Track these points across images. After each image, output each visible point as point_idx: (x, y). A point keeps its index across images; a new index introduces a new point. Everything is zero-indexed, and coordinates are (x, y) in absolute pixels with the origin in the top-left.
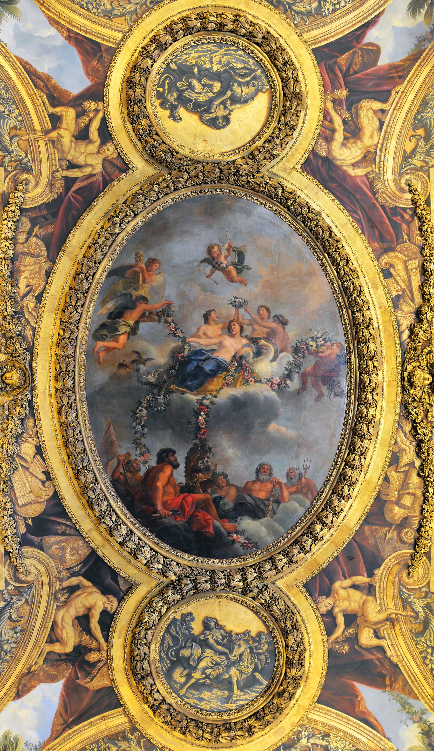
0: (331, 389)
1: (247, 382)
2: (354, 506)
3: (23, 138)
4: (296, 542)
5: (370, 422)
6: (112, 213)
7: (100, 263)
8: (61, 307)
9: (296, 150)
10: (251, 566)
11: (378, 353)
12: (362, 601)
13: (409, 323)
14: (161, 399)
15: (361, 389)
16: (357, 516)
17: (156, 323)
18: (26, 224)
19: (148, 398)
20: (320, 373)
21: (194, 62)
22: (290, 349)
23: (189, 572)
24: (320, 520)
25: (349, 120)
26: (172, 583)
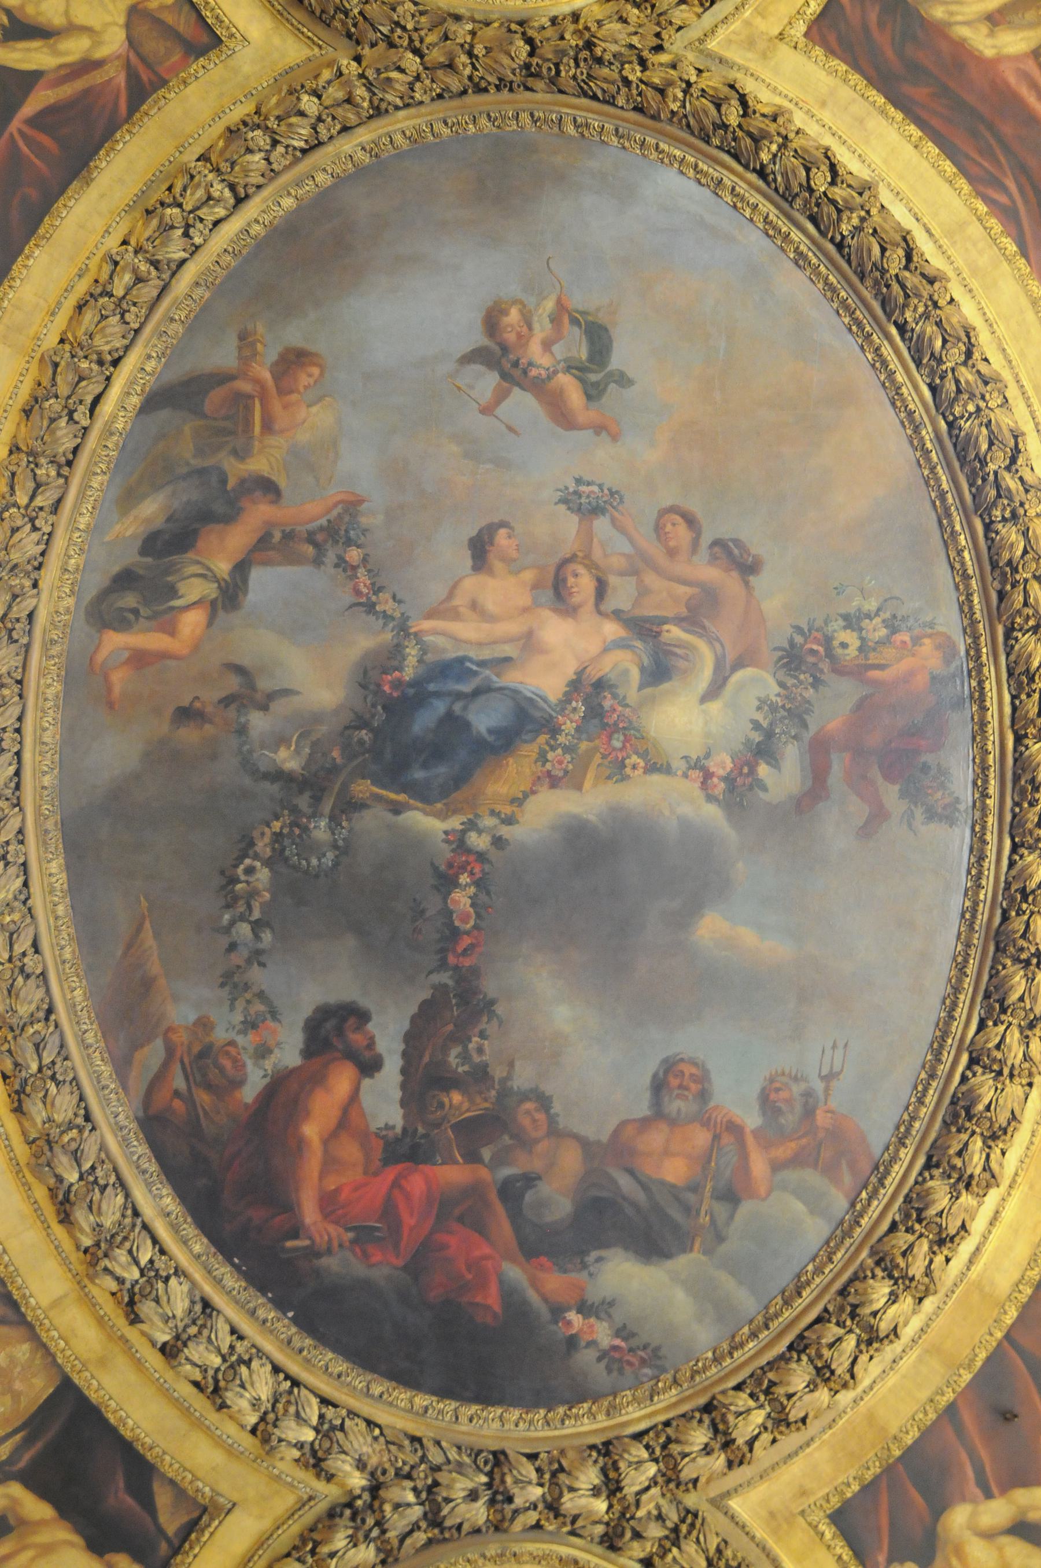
0: (913, 793)
1: (618, 771)
2: (1009, 1214)
4: (799, 1347)
6: (160, 193)
7: (115, 363)
10: (638, 1436)
15: (1023, 792)
19: (277, 825)
24: (884, 1262)
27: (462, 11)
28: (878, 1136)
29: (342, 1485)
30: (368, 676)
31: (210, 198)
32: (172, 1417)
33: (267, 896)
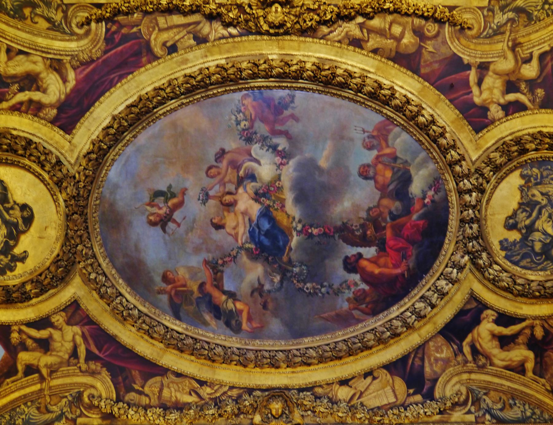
0: (286, 107)
1: (280, 189)
2: (400, 84)
3: (49, 400)
4: (435, 141)
5: (318, 68)
6: (119, 317)
7: (167, 328)
8: (209, 363)
10: (457, 184)
12: (495, 76)
13: (221, 27)
14: (296, 270)
16: (410, 80)
18: (131, 396)
19: (295, 282)
20: (271, 117)
23: (462, 243)
25: (20, 86)
26: (471, 260)
27: (65, 233)
28: (379, 118)
29: (467, 261)
30: (253, 256)
31: (120, 303)
32: (449, 305)
33: (314, 284)
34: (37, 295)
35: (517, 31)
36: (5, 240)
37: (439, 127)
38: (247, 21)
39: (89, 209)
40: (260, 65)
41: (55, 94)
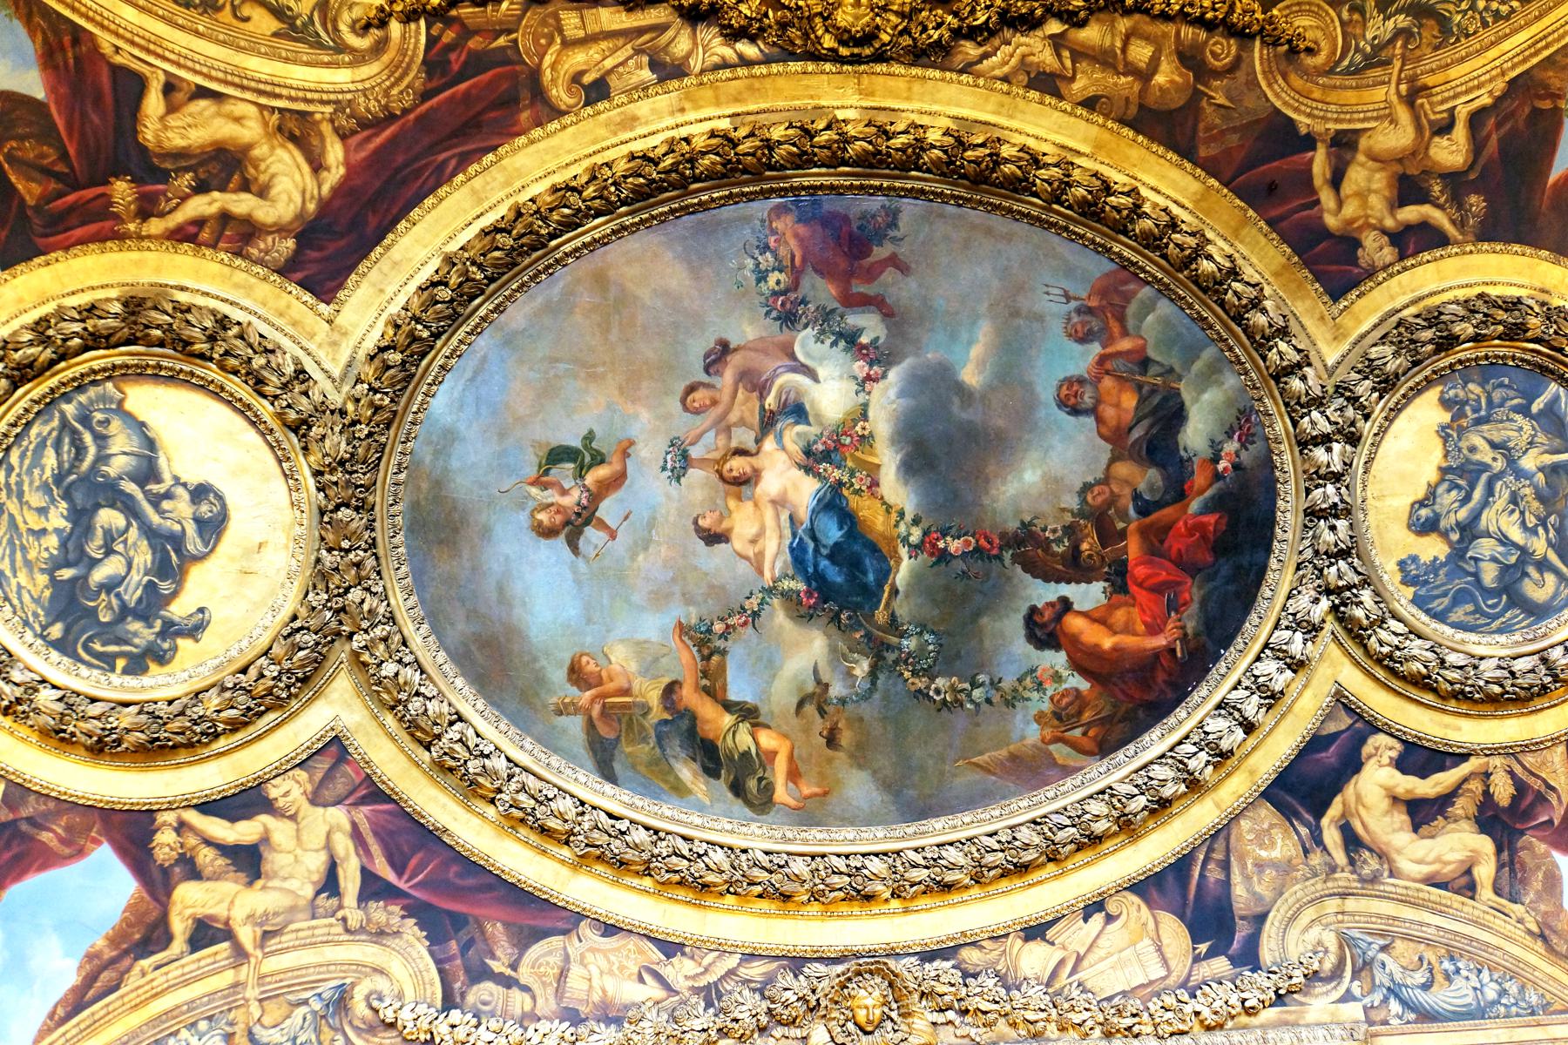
0: (880, 236)
1: (866, 440)
2: (1153, 182)
3: (256, 1013)
4: (1238, 318)
5: (959, 140)
7: (583, 804)
9: (281, 315)
10: (1295, 424)
11: (796, 118)
13: (719, 39)
14: (910, 644)
15: (881, 162)
16: (1175, 174)
17: (728, 658)
18: (486, 990)
19: (907, 674)
20: (843, 264)
21: (43, 579)
22: (786, 335)
26: (1334, 609)
28: (1100, 267)
30: (803, 613)
31: (460, 740)
34: (235, 726)
35: (1419, 59)
36: (146, 578)
37: (1248, 284)
38: (783, 26)
39: (379, 493)
40: (818, 132)
41: (290, 200)
